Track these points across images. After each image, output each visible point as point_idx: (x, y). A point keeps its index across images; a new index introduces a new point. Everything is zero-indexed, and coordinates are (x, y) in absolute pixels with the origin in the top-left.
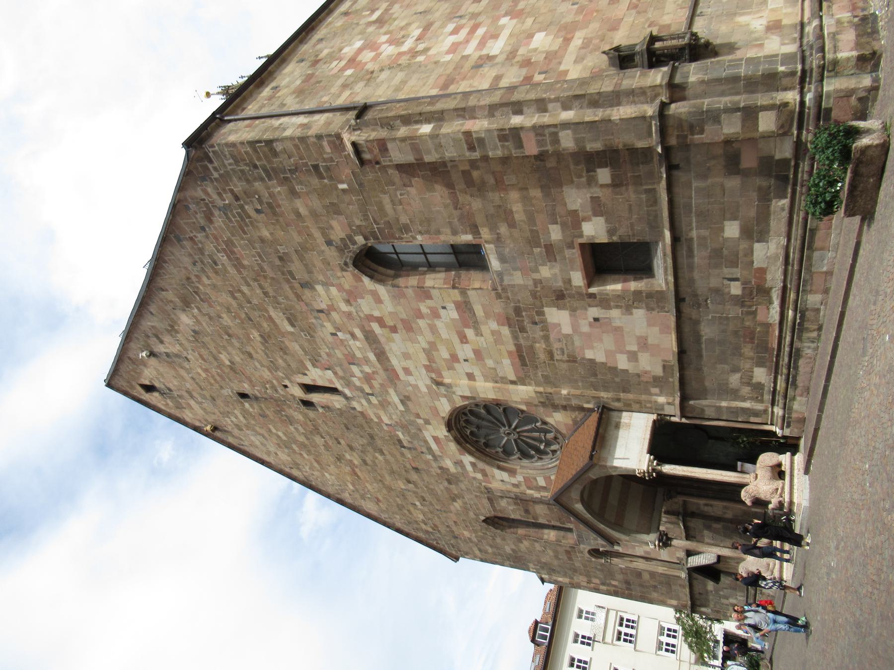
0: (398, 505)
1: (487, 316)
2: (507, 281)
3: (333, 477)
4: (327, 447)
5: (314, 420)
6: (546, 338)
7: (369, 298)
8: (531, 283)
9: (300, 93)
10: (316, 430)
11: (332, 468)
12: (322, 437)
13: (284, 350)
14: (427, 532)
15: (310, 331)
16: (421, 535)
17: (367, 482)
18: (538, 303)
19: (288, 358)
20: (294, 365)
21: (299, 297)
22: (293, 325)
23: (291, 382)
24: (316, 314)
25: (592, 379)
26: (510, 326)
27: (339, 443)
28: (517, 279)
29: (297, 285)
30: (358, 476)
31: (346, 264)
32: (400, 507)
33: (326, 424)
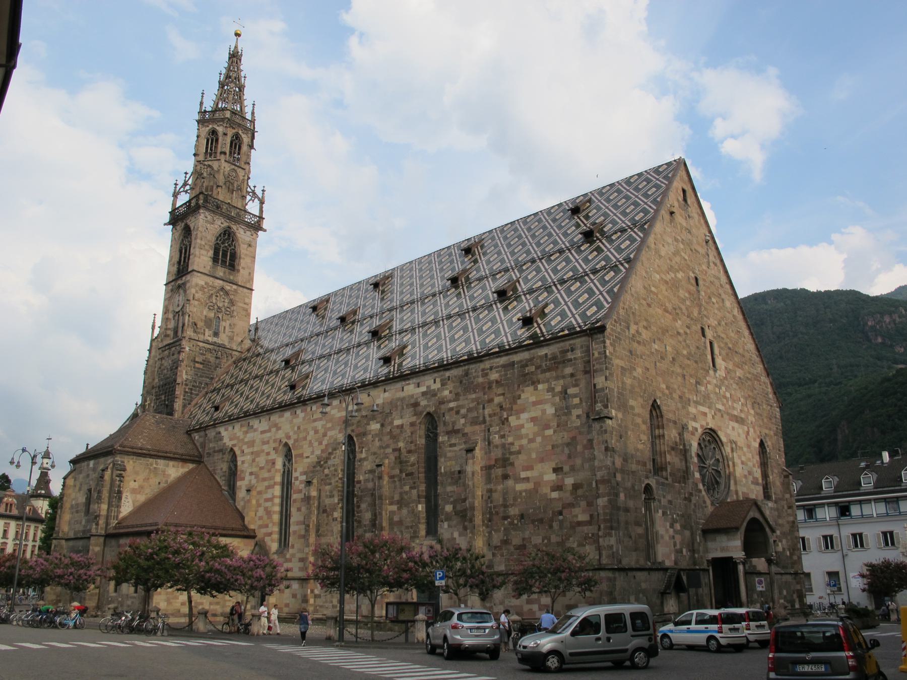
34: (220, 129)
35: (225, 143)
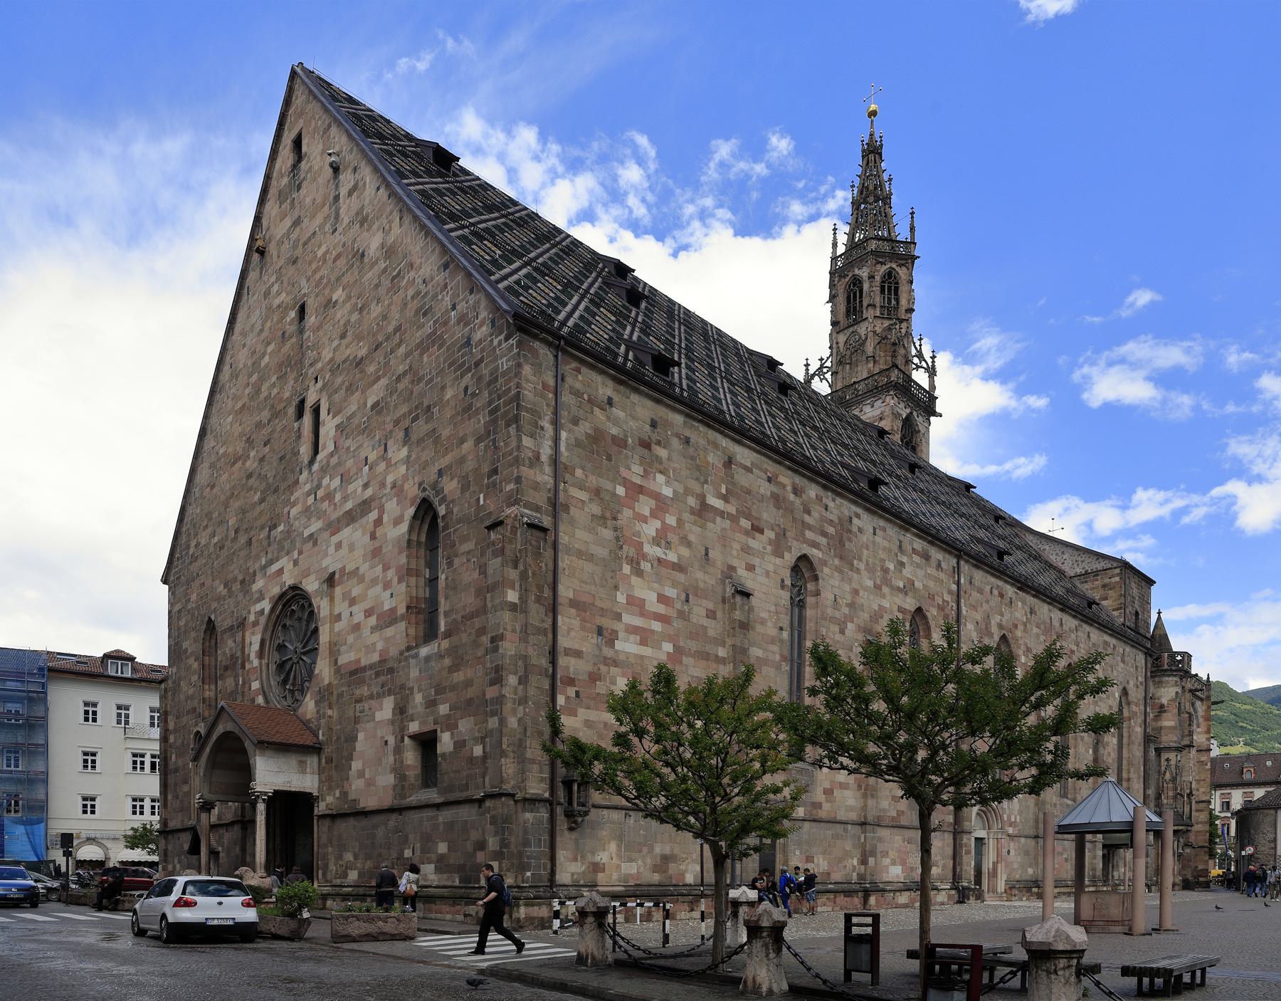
0: (210, 513)
1: (387, 640)
2: (412, 661)
3: (229, 427)
4: (259, 425)
5: (285, 414)
6: (371, 697)
7: (397, 513)
8: (411, 685)
9: (597, 436)
10: (276, 415)
11: (238, 429)
12: (269, 421)
13: (350, 389)
14: (188, 547)
15: (366, 430)
16: (184, 538)
17: (230, 476)
18: (397, 690)
19: (343, 391)
20: (337, 397)
21: (397, 422)
22: (373, 407)
23: (321, 390)
24: (383, 442)
25: (343, 739)
26: (380, 662)
27: (265, 445)
28: (414, 673)
29: (407, 423)
30: (234, 463)
31: (424, 490)
32: (209, 515)
33: (283, 430)
34: (864, 273)
35: (872, 292)
